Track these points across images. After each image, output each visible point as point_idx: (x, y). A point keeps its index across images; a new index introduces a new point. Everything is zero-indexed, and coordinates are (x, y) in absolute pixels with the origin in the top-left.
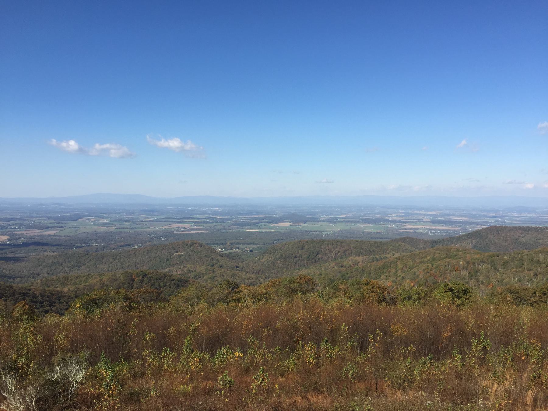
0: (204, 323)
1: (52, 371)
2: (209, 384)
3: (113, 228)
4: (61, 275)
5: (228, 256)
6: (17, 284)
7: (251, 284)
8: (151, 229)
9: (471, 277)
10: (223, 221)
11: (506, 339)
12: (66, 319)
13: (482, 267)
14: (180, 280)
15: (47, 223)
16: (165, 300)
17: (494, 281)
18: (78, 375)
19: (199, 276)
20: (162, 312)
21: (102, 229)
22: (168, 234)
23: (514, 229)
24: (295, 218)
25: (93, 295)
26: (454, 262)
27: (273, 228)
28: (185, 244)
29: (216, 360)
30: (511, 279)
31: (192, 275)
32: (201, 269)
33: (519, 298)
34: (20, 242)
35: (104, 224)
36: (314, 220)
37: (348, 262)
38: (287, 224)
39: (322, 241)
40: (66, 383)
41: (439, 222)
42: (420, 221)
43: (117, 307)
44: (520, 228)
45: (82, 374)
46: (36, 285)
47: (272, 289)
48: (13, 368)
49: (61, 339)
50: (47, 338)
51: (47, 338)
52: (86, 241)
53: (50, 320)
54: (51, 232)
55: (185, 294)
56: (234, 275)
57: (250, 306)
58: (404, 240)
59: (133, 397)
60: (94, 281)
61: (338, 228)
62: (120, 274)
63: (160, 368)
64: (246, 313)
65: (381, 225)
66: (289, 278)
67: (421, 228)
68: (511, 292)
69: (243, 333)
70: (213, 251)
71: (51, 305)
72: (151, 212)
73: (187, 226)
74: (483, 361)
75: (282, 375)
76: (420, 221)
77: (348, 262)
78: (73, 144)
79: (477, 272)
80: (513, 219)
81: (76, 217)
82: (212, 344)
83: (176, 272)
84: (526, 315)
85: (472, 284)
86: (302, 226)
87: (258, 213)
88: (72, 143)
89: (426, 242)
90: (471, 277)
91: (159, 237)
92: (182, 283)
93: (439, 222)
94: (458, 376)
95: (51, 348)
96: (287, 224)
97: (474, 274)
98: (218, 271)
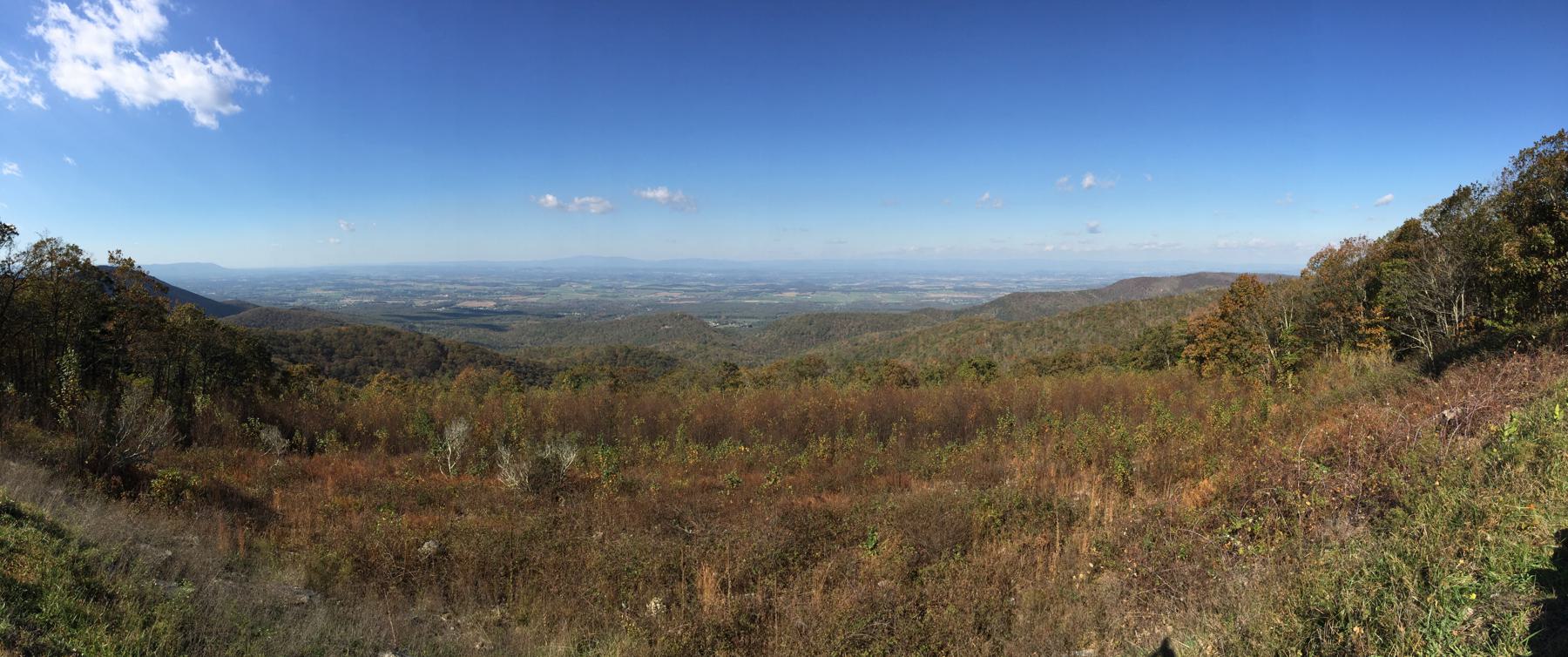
0: (699, 410)
1: (543, 449)
2: (707, 480)
3: (594, 296)
4: (544, 346)
5: (723, 332)
6: (503, 354)
7: (750, 366)
8: (635, 299)
9: (994, 350)
10: (717, 289)
11: (1029, 413)
12: (552, 394)
13: (1006, 338)
14: (669, 359)
15: (530, 288)
16: (652, 380)
17: (1017, 352)
18: (570, 457)
19: (689, 354)
20: (650, 395)
21: (584, 297)
22: (655, 304)
23: (1035, 295)
24: (802, 286)
25: (578, 370)
26: (977, 334)
27: (776, 299)
28: (674, 317)
29: (718, 452)
30: (1033, 350)
31: (681, 353)
32: (692, 346)
33: (1042, 368)
34: (505, 308)
35: (587, 291)
36: (824, 289)
37: (863, 339)
38: (793, 294)
39: (834, 315)
40: (557, 461)
41: (962, 290)
42: (942, 289)
43: (603, 385)
44: (1042, 294)
45: (573, 457)
46: (521, 355)
47: (776, 372)
48: (507, 441)
49: (549, 417)
50: (535, 413)
51: (535, 413)
52: (569, 309)
53: (537, 393)
54: (534, 299)
55: (676, 375)
56: (729, 355)
57: (750, 393)
58: (925, 311)
59: (628, 488)
60: (576, 354)
61: (852, 298)
62: (602, 348)
63: (652, 458)
64: (746, 399)
65: (901, 294)
66: (796, 359)
67: (944, 297)
68: (1033, 362)
69: (745, 424)
70: (706, 325)
71: (535, 376)
72: (634, 278)
73: (675, 295)
74: (1009, 440)
75: (792, 473)
76: (942, 289)
77: (863, 339)
78: (550, 199)
79: (1000, 343)
80: (1035, 285)
81: (557, 284)
82: (711, 435)
83: (664, 349)
84: (1048, 385)
85: (995, 358)
86: (810, 297)
87: (759, 280)
88: (550, 198)
89: (948, 313)
90: (994, 350)
91: (645, 307)
92: (669, 363)
93: (962, 290)
94: (985, 458)
95: (540, 422)
96: (793, 294)
97: (998, 346)
98: (712, 350)
